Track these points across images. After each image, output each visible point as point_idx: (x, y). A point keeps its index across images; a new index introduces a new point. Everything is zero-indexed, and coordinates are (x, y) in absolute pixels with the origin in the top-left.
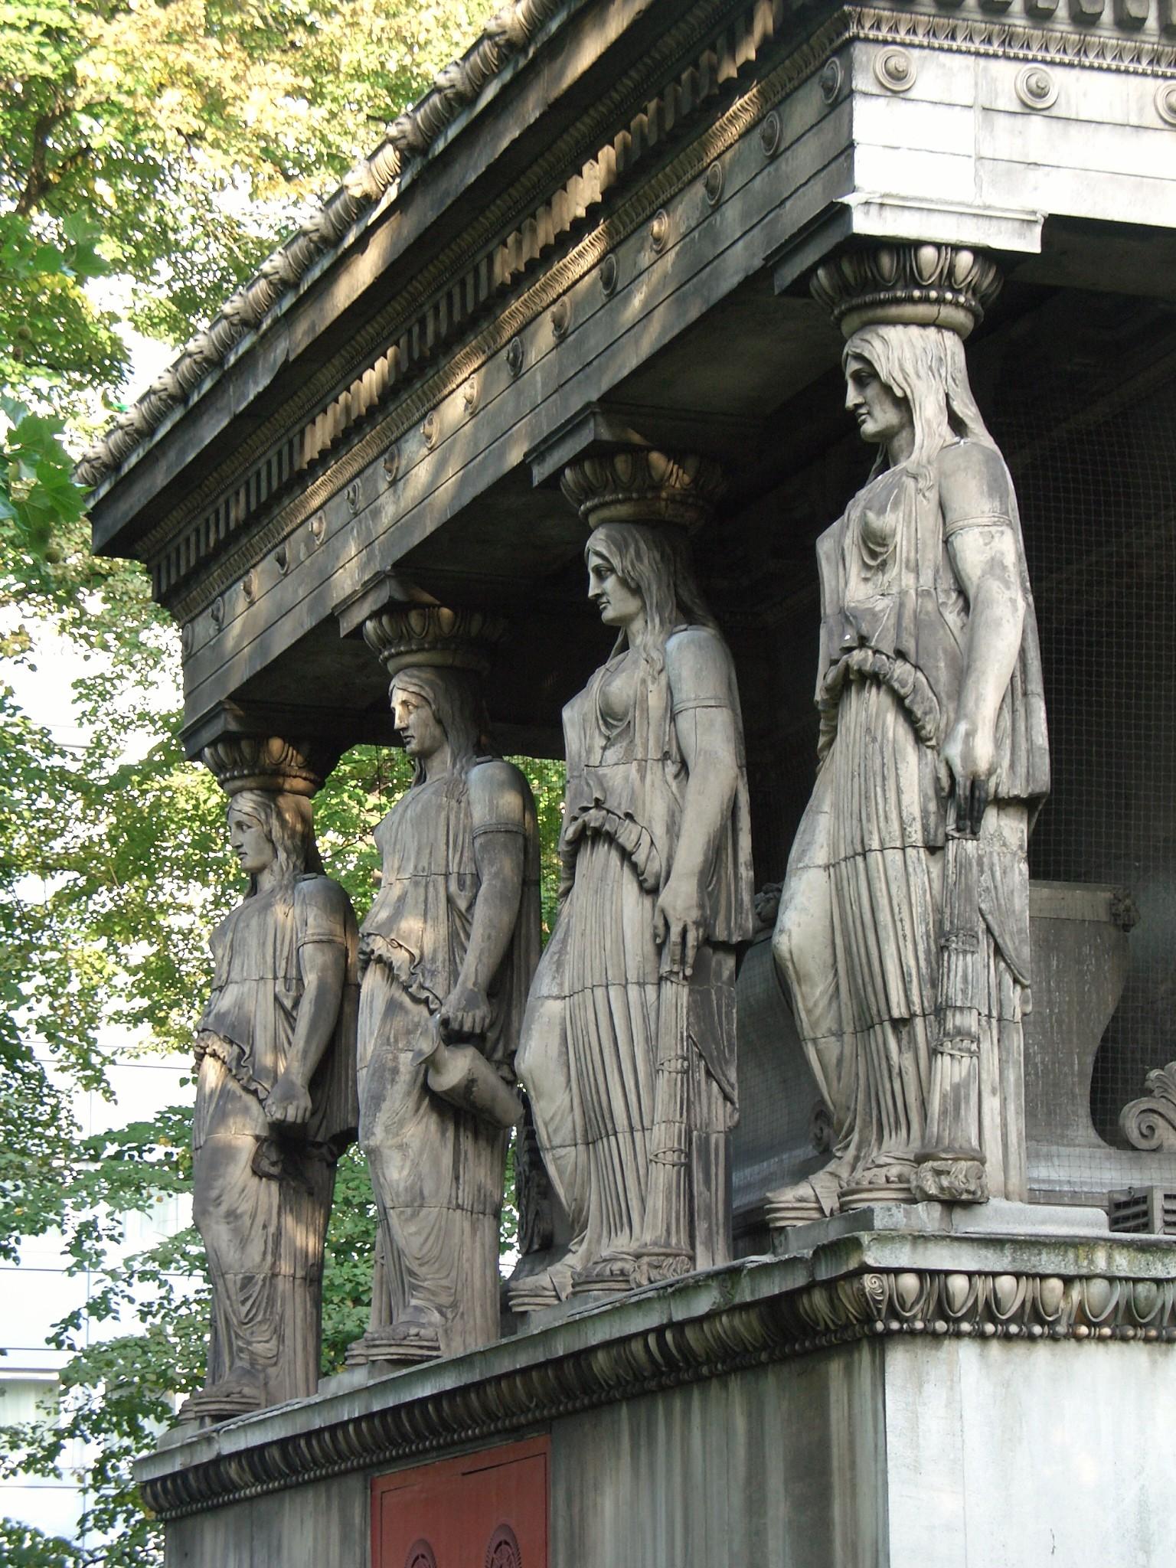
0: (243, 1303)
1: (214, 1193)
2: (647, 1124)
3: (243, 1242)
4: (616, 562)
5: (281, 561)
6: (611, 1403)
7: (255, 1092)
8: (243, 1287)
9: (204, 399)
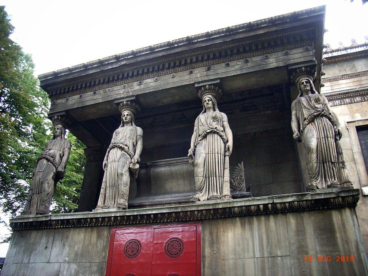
0: (46, 197)
1: (47, 178)
2: (222, 176)
3: (49, 188)
4: (213, 100)
5: (95, 93)
6: (236, 217)
7: (55, 166)
8: (47, 195)
9: (122, 60)
